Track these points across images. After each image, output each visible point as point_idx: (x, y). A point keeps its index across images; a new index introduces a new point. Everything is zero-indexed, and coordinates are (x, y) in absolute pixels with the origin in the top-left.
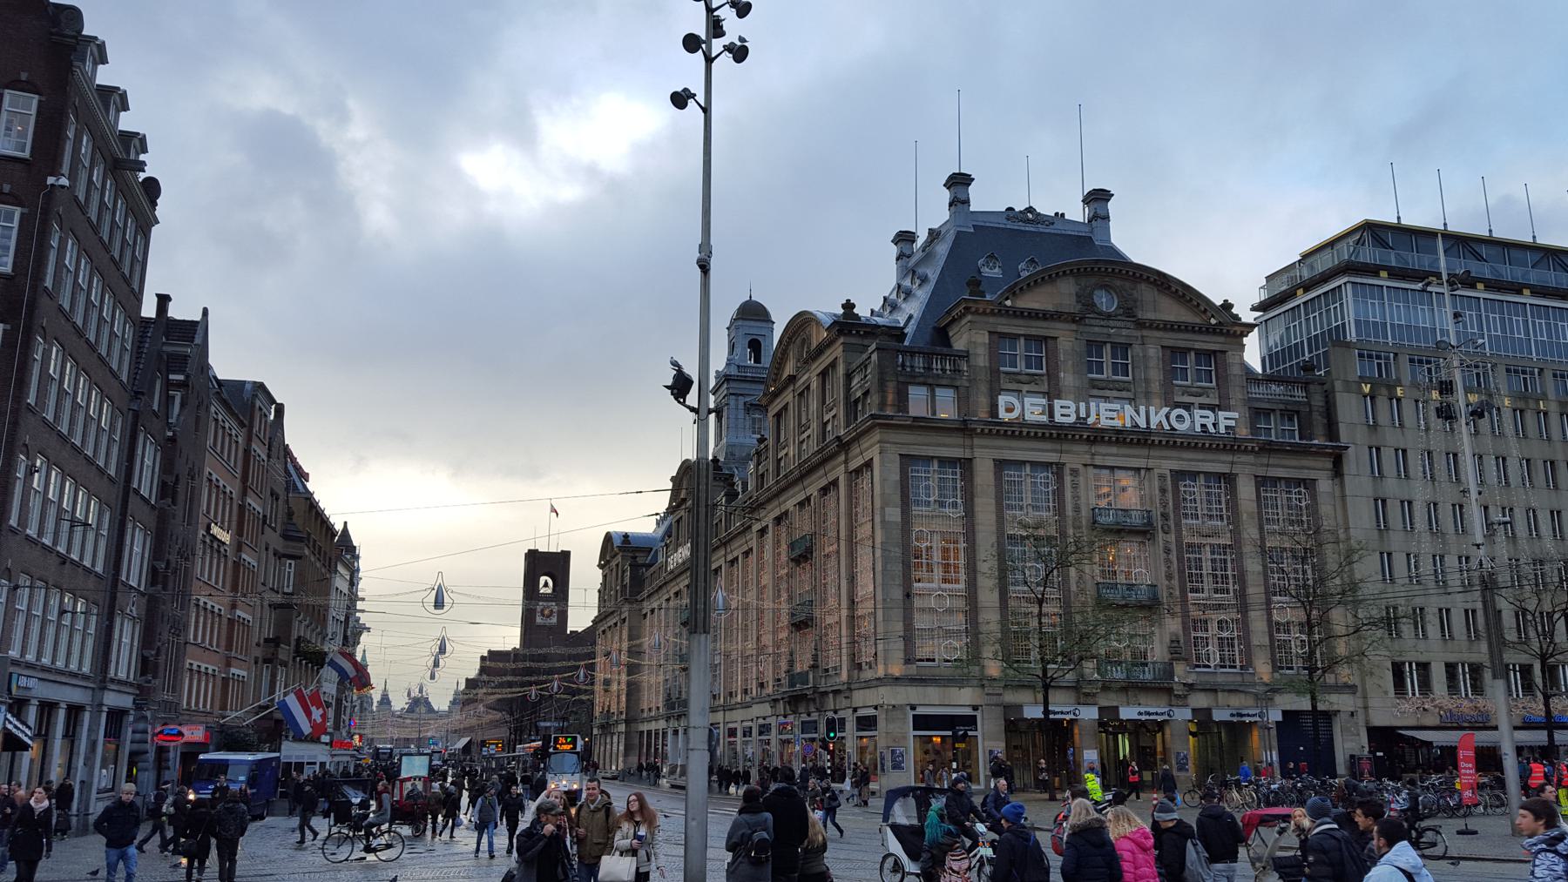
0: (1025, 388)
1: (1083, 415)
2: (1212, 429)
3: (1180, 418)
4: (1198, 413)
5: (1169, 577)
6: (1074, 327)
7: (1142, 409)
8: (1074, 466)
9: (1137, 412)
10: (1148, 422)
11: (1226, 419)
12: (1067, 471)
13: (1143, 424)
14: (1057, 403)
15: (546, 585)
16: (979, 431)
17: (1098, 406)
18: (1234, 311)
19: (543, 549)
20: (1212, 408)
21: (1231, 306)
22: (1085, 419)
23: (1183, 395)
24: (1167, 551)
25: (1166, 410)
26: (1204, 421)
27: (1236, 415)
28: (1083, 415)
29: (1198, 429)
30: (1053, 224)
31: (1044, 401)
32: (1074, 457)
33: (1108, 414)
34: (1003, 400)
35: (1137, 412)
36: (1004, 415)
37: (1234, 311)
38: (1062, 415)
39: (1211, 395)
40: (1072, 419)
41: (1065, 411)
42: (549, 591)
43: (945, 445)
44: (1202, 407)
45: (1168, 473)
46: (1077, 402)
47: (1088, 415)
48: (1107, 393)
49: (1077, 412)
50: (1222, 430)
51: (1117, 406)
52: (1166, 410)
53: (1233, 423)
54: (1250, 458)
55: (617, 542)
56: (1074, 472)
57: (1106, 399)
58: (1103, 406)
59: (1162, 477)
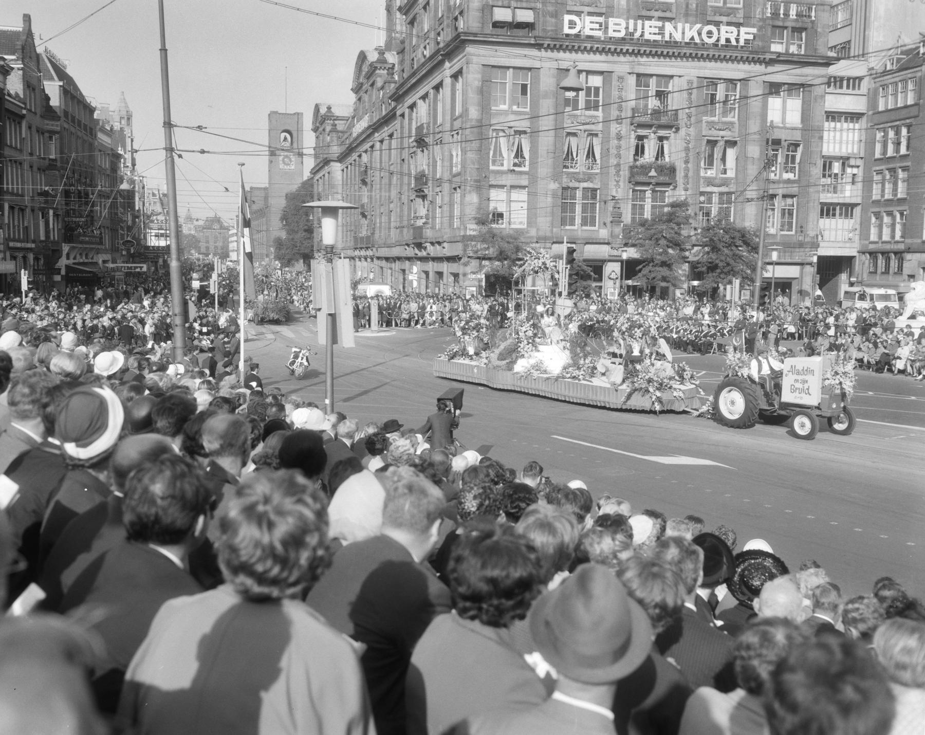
0: (587, 9)
1: (631, 29)
2: (734, 43)
3: (710, 33)
4: (723, 28)
5: (687, 162)
7: (680, 26)
8: (621, 74)
9: (675, 28)
10: (683, 38)
11: (747, 33)
12: (615, 77)
13: (678, 37)
14: (611, 21)
15: (285, 139)
16: (545, 46)
17: (643, 25)
19: (282, 110)
20: (738, 25)
22: (632, 34)
23: (715, 15)
26: (728, 35)
27: (754, 30)
28: (631, 29)
29: (723, 42)
31: (601, 19)
32: (621, 65)
33: (649, 30)
34: (567, 18)
35: (675, 28)
36: (567, 30)
39: (737, 16)
40: (622, 34)
41: (617, 28)
42: (288, 144)
43: (516, 56)
44: (729, 24)
45: (695, 80)
46: (628, 19)
47: (635, 30)
48: (653, 13)
49: (627, 28)
50: (742, 43)
51: (660, 24)
52: (698, 26)
53: (751, 37)
55: (323, 110)
56: (621, 78)
57: (650, 18)
58: (647, 23)
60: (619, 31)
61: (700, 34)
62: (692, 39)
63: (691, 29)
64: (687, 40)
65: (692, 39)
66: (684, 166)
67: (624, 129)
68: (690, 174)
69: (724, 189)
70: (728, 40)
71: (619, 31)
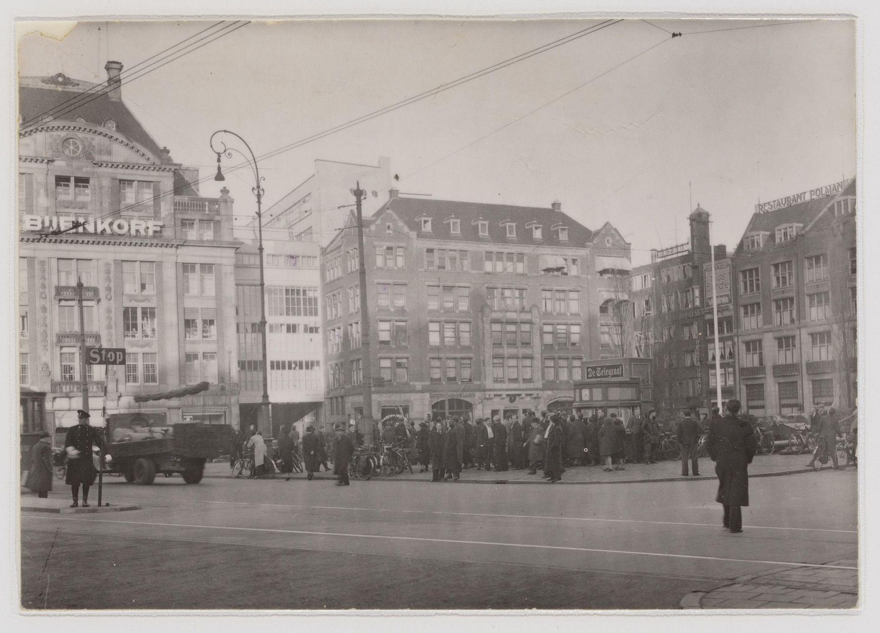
2: (143, 233)
3: (120, 227)
6: (44, 165)
10: (96, 229)
18: (170, 155)
21: (168, 152)
24: (109, 311)
25: (109, 220)
26: (137, 228)
28: (47, 224)
29: (133, 232)
30: (78, 85)
37: (170, 155)
38: (32, 225)
40: (39, 227)
49: (43, 223)
53: (158, 229)
54: (172, 251)
59: (108, 264)
60: (36, 226)
61: (111, 224)
62: (104, 230)
63: (102, 223)
64: (99, 230)
65: (104, 230)
66: (107, 332)
67: (48, 303)
68: (114, 338)
69: (147, 350)
70: (137, 231)
71: (36, 226)
